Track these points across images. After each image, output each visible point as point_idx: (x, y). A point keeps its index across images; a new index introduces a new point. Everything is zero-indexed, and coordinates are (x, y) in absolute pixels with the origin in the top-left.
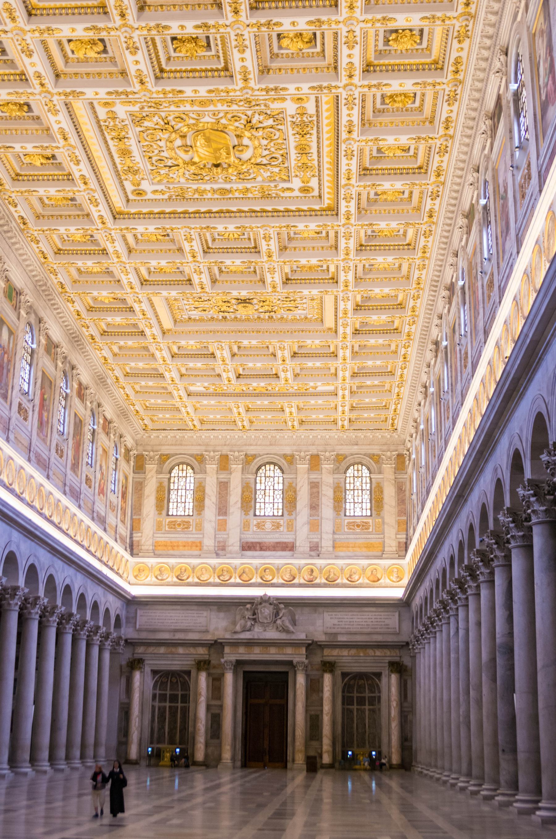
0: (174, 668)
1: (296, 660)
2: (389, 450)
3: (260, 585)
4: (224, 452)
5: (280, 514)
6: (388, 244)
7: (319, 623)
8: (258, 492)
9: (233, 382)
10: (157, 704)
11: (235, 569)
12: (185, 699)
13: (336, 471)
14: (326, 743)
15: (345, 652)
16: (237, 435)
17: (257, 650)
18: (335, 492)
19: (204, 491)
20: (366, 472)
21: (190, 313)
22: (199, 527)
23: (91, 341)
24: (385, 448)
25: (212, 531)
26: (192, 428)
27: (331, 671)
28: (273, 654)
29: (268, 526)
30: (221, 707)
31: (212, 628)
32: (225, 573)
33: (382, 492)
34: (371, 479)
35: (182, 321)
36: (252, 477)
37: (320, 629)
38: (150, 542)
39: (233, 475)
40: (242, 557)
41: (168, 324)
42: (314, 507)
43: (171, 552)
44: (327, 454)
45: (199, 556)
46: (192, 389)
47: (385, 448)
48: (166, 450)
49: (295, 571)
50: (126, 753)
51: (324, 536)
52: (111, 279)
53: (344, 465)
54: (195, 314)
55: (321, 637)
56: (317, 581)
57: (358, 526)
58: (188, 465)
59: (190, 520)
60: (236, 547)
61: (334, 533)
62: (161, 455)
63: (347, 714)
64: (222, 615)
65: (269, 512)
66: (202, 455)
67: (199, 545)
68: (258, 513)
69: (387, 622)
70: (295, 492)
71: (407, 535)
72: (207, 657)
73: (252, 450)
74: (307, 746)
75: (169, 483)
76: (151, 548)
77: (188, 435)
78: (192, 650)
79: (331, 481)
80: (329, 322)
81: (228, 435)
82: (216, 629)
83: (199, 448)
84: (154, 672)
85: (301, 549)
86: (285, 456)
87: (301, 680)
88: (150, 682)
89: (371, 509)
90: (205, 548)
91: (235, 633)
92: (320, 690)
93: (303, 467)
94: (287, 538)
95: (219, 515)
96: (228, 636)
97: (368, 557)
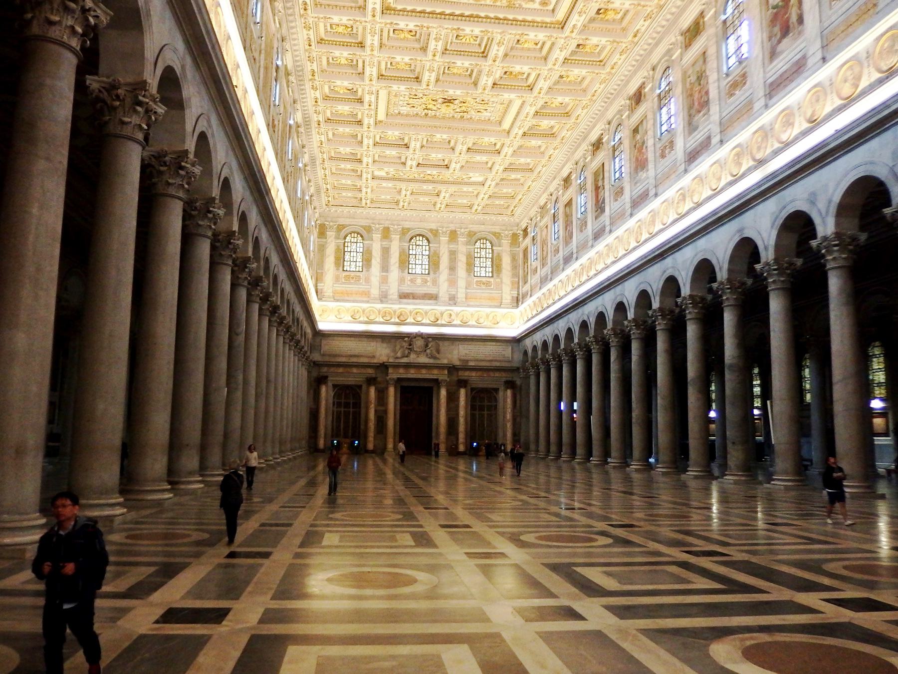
0: (350, 383)
1: (440, 378)
2: (506, 230)
3: (413, 324)
4: (386, 226)
5: (427, 273)
6: (586, 59)
7: (455, 352)
8: (411, 256)
9: (413, 169)
10: (335, 409)
11: (395, 312)
12: (357, 405)
13: (468, 243)
14: (461, 437)
15: (474, 374)
16: (397, 212)
17: (412, 371)
18: (467, 258)
19: (371, 253)
20: (489, 245)
21: (403, 108)
22: (368, 280)
23: (317, 126)
24: (504, 228)
25: (377, 284)
26: (364, 205)
27: (465, 387)
28: (424, 374)
29: (419, 281)
30: (386, 412)
31: (378, 354)
32: (387, 315)
33: (501, 260)
34: (492, 250)
35: (392, 115)
36: (407, 244)
37: (456, 357)
38: (330, 291)
39: (393, 242)
40: (400, 303)
41: (381, 116)
42: (452, 268)
43: (347, 298)
44: (462, 230)
45: (368, 302)
46: (377, 173)
47: (504, 228)
48: (342, 221)
49: (438, 315)
50: (316, 443)
51: (459, 290)
52: (354, 72)
53: (474, 239)
54: (405, 110)
55: (457, 363)
56: (454, 323)
57: (484, 284)
58: (358, 234)
59: (361, 274)
60: (396, 297)
61: (466, 288)
62: (339, 225)
63: (473, 416)
64: (385, 345)
65: (419, 271)
66: (370, 227)
67: (367, 294)
68: (410, 272)
69: (504, 353)
70: (439, 257)
71: (518, 291)
72: (374, 376)
73: (407, 225)
74: (447, 439)
75: (344, 246)
76: (331, 294)
77: (360, 210)
78: (363, 371)
79: (465, 250)
80: (506, 125)
81: (391, 212)
82: (381, 355)
83: (367, 221)
84: (335, 386)
85: (443, 299)
86: (431, 230)
87: (443, 392)
88: (332, 393)
89: (492, 272)
90: (372, 296)
91: (397, 358)
92: (457, 399)
93: (444, 239)
94: (432, 290)
95: (383, 272)
96: (391, 360)
97: (490, 307)
